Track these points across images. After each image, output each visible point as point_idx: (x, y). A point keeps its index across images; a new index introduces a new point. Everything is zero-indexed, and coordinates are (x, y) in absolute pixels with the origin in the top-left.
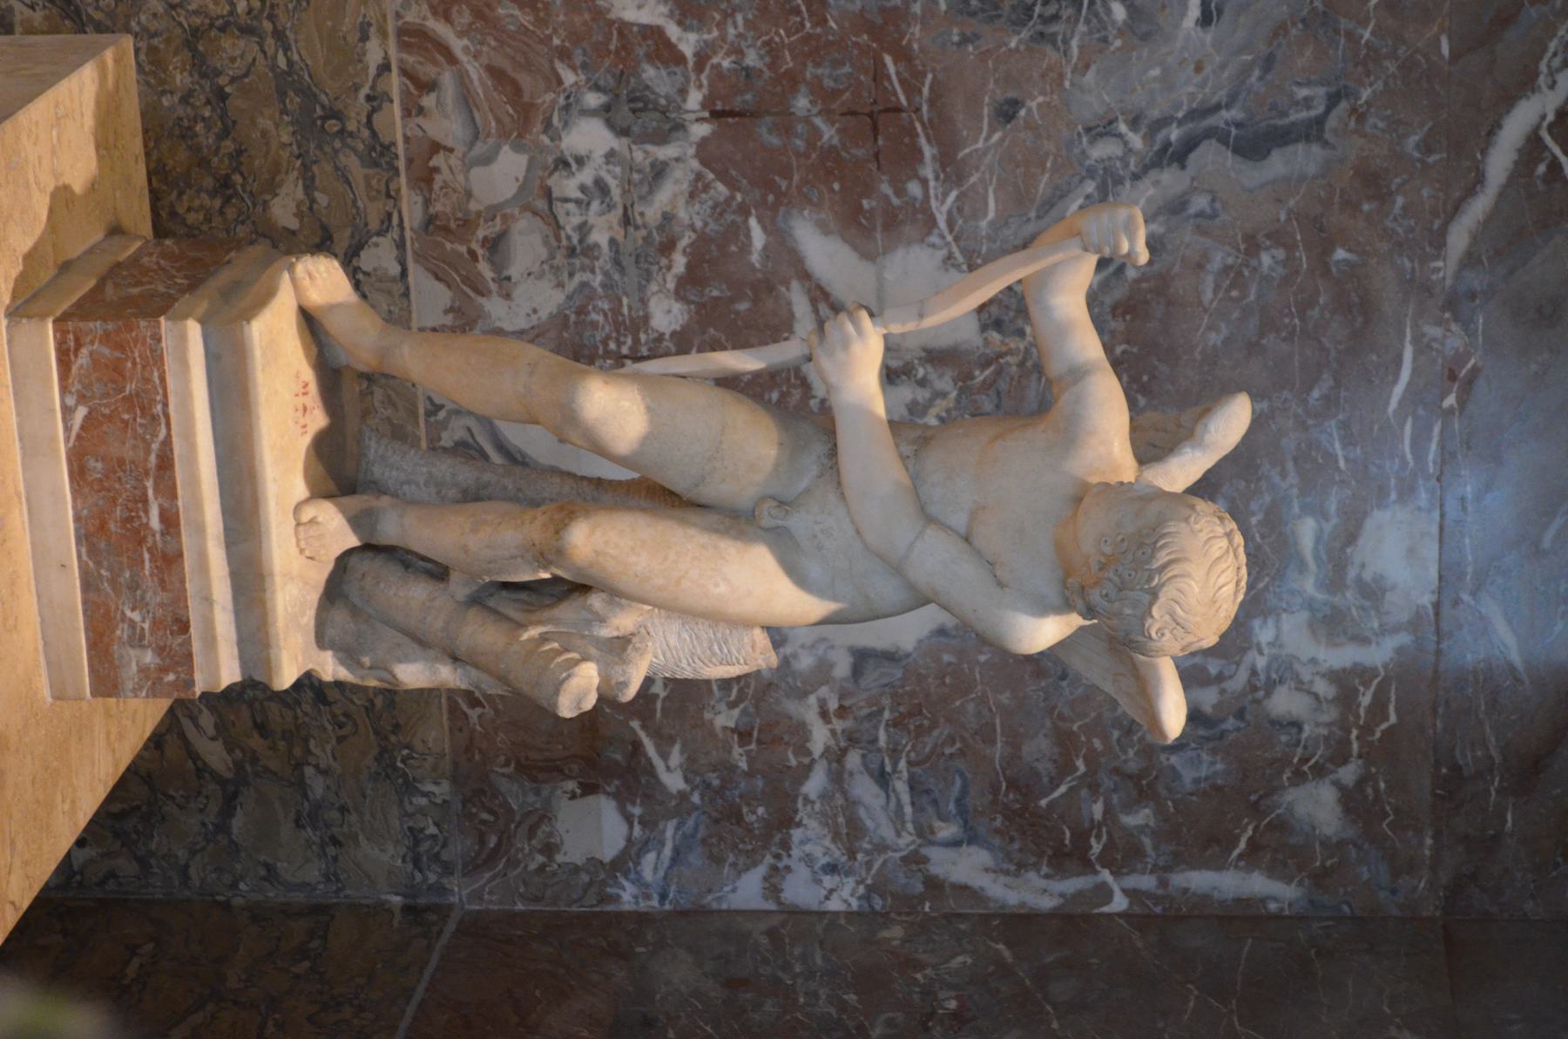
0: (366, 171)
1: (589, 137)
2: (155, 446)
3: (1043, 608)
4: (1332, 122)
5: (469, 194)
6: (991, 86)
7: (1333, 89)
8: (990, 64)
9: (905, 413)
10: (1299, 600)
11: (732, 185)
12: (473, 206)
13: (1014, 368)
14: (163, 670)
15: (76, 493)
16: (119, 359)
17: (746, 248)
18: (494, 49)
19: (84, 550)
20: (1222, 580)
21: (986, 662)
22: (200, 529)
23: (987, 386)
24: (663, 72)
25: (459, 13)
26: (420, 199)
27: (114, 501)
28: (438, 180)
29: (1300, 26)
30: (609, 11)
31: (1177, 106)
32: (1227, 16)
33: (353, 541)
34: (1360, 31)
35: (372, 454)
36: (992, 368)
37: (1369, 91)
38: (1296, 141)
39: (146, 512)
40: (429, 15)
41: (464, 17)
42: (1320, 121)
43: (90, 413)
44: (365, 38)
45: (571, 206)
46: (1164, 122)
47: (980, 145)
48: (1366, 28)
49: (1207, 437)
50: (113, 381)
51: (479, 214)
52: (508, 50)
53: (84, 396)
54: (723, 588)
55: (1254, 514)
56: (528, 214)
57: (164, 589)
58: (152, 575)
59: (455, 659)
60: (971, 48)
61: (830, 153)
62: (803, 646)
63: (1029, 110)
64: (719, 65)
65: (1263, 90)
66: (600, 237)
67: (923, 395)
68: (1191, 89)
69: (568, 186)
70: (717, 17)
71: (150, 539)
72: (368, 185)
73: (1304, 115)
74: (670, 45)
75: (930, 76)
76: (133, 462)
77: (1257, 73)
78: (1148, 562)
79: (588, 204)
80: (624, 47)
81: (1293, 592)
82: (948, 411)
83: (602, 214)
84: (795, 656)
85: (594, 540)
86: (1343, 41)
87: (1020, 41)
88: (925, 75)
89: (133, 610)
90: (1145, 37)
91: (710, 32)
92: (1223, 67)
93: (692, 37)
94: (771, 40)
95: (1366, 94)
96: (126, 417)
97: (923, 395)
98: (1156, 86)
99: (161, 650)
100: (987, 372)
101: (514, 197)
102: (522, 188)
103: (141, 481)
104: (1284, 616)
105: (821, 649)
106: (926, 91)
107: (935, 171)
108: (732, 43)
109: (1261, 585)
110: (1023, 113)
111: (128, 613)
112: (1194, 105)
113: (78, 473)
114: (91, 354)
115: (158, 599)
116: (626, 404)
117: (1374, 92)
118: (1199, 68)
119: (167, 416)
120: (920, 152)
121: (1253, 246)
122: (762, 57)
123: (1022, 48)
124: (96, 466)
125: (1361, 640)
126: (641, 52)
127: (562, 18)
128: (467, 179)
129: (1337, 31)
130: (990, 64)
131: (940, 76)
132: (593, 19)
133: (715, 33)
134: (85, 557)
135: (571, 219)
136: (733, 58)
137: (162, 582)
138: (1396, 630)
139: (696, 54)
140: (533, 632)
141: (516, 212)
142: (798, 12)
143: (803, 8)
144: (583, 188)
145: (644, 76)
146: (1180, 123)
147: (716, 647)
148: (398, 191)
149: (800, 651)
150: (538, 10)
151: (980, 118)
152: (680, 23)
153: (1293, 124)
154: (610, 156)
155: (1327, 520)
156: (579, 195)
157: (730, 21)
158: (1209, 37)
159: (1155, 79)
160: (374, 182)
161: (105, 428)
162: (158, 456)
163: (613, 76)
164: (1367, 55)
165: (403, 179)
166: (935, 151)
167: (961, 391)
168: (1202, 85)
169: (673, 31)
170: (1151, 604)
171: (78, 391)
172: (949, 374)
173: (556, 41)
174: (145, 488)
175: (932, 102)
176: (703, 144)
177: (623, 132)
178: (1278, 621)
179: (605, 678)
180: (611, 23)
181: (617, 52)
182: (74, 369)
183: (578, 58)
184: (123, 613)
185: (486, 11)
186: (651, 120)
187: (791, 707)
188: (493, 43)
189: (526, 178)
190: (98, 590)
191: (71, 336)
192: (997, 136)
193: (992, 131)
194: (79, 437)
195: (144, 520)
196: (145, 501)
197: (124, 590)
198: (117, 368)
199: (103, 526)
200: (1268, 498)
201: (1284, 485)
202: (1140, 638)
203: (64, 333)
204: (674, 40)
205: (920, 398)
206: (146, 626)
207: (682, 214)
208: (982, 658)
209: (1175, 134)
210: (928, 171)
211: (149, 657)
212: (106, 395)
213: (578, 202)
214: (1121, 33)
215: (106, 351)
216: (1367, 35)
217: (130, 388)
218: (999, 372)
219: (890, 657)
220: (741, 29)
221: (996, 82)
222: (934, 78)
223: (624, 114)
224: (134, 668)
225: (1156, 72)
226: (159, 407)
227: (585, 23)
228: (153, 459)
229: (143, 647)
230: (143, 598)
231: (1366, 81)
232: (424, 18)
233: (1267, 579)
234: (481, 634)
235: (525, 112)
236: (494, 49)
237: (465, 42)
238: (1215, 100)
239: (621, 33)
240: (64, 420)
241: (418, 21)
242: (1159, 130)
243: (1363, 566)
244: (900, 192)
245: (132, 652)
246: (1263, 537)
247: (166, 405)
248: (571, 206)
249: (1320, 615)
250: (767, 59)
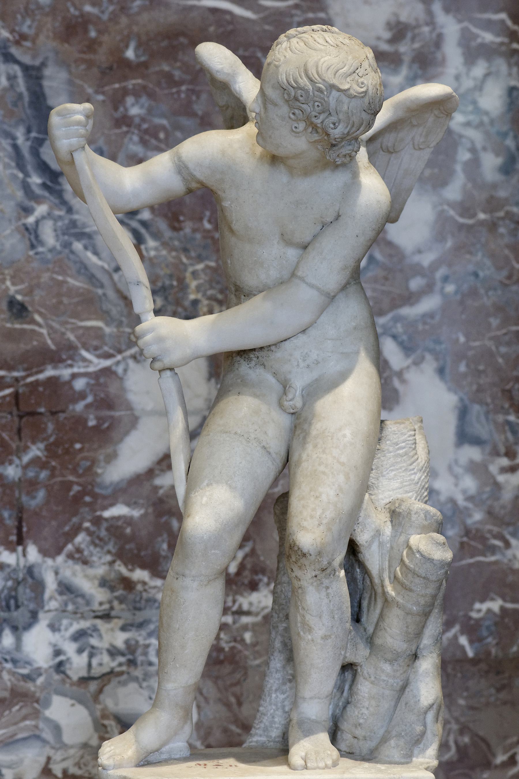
1: (38, 644)
3: (353, 185)
4: (27, 60)
11: (77, 530)
17: (128, 521)
20: (321, 41)
31: (15, 177)
33: (324, 737)
35: (263, 739)
38: (41, 86)
42: (26, 68)
45: (95, 662)
47: (44, 331)
49: (226, 71)
54: (347, 432)
56: (102, 697)
59: (415, 657)
61: (51, 450)
62: (456, 485)
66: (120, 639)
69: (78, 663)
78: (307, 91)
79: (93, 647)
83: (100, 636)
84: (464, 492)
85: (312, 526)
101: (87, 707)
102: (81, 702)
105: (459, 470)
110: (19, 297)
112: (13, 164)
116: (205, 499)
121: (125, 121)
125: (438, 42)
128: (72, 747)
135: (105, 662)
138: (430, 13)
140: (390, 590)
141: (99, 707)
144: (80, 651)
146: (27, 175)
147: (401, 452)
151: (24, 331)
153: (28, 89)
154: (53, 627)
156: (85, 655)
166: (49, 367)
170: (339, 90)
175: (10, 368)
176: (44, 552)
177: (34, 617)
179: (424, 530)
186: (25, 593)
187: (507, 496)
189: (72, 698)
192: (37, 318)
193: (33, 322)
202: (366, 100)
207: (101, 571)
208: (462, 339)
209: (36, 180)
210: (65, 373)
213: (91, 656)
219: (463, 413)
223: (20, 615)
234: (393, 633)
235: (18, 695)
238: (9, 149)
242: (32, 192)
243: (379, 38)
244: (82, 395)
248: (95, 662)
249: (420, 72)
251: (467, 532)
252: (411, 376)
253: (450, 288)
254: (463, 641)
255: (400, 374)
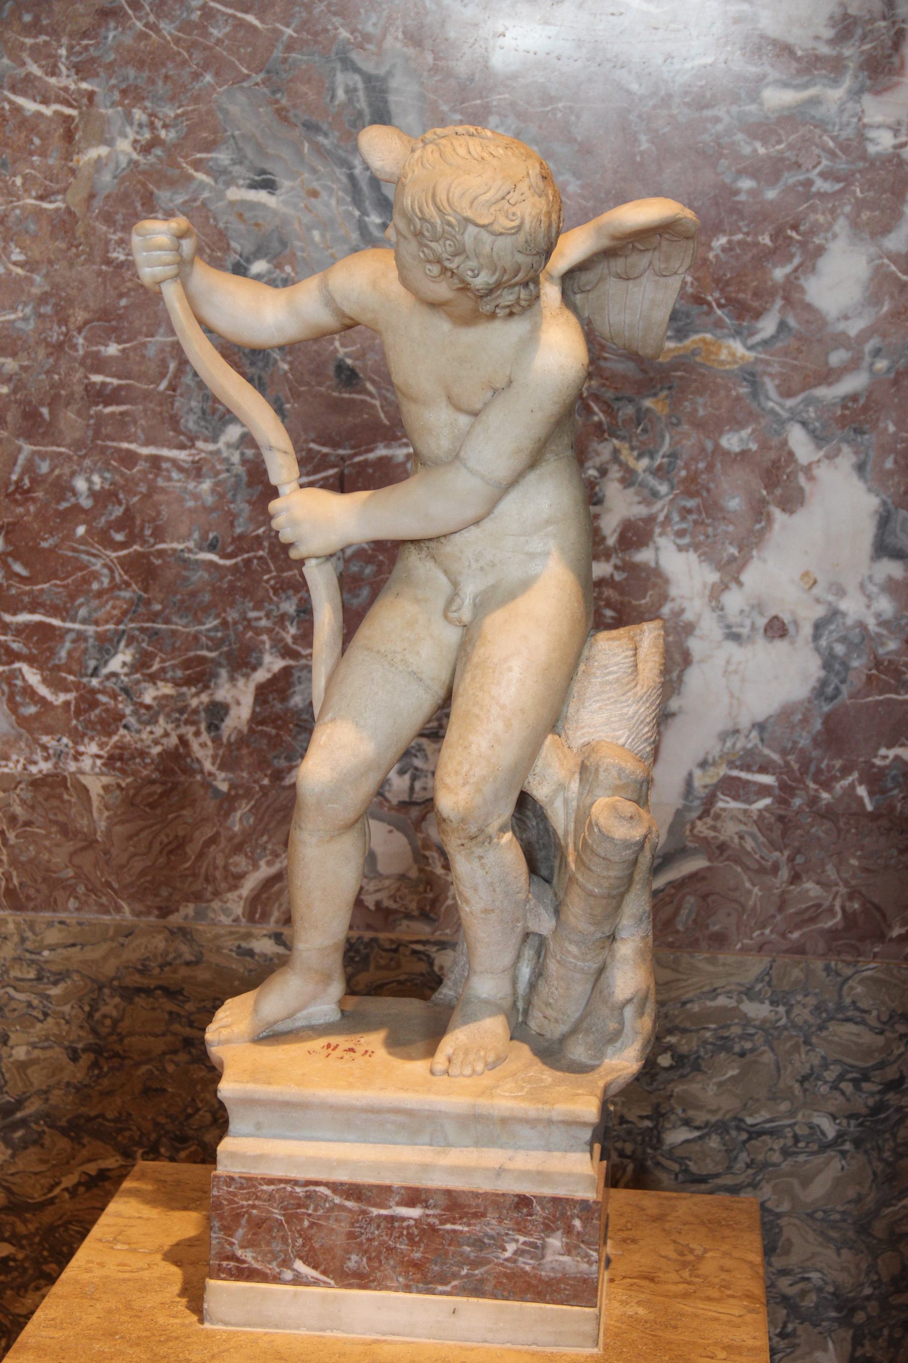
0: (372, 967)
2: (337, 1200)
3: (531, 340)
5: (402, 877)
6: (323, 389)
7: (339, 66)
8: (302, 389)
9: (631, 490)
10: (850, 105)
12: (414, 874)
13: (593, 383)
14: (569, 1230)
15: (381, 1287)
16: (248, 1221)
18: (270, 838)
19: (440, 1288)
20: (462, 151)
21: (895, 424)
22: (425, 1168)
23: (609, 410)
24: (298, 688)
25: (236, 865)
26: (405, 923)
27: (390, 1249)
28: (387, 903)
29: (278, 96)
30: (240, 732)
31: (350, 215)
32: (268, 166)
34: (285, 38)
35: (452, 993)
36: (592, 404)
37: (341, 30)
38: (386, 102)
39: (403, 1219)
40: (237, 893)
41: (240, 862)
43: (301, 1258)
44: (250, 953)
45: (418, 785)
46: (362, 227)
47: (377, 403)
48: (282, 33)
49: (388, 169)
50: (270, 1230)
51: (421, 870)
52: (272, 826)
53: (284, 1261)
55: (755, 151)
56: (423, 825)
57: (483, 1215)
58: (469, 1225)
59: (612, 938)
60: (288, 406)
62: (868, 607)
63: (347, 355)
64: (294, 637)
65: (337, 134)
67: (615, 472)
68: (333, 202)
70: (250, 634)
71: (431, 1220)
72: (386, 967)
73: (361, 94)
74: (274, 679)
75: (312, 445)
76: (352, 1225)
77: (321, 139)
78: (433, 226)
79: (416, 769)
80: (274, 721)
81: (842, 111)
82: (632, 448)
83: (426, 757)
84: (878, 615)
86: (293, 55)
87: (283, 360)
88: (310, 450)
89: (504, 1250)
90: (284, 243)
91: (263, 643)
92: (314, 171)
93: (267, 659)
94: (273, 588)
95: (344, 34)
96: (306, 1223)
97: (615, 472)
98: (328, 236)
99: (548, 1228)
100: (596, 409)
101: (407, 835)
102: (399, 828)
103: (371, 1219)
104: (866, 120)
105: (873, 589)
106: (325, 450)
107: (400, 446)
108: (275, 623)
109: (831, 144)
110: (349, 361)
111: (507, 1254)
112: (349, 199)
113: (362, 1280)
114: (242, 1247)
115: (494, 1222)
116: (324, 738)
117: (342, 25)
118: (314, 194)
119: (308, 1183)
120: (381, 459)
122: (288, 598)
123: (289, 358)
124: (354, 1261)
126: (279, 706)
127: (245, 774)
128: (387, 877)
129: (285, 61)
130: (302, 389)
131: (313, 435)
132: (248, 746)
133: (265, 637)
134: (448, 1288)
136: (288, 623)
137: (475, 1215)
139: (283, 656)
141: (420, 835)
142: (248, 562)
143: (246, 556)
144: (401, 772)
145: (301, 705)
146: (364, 213)
147: (611, 677)
148: (392, 941)
149: (873, 610)
150: (237, 795)
151: (353, 401)
152: (254, 669)
153: (370, 105)
155: (765, 76)
156: (407, 777)
157: (254, 624)
158: (286, 183)
159: (323, 236)
160: (382, 962)
161: (317, 1246)
162: (347, 1199)
163: (299, 733)
164: (308, 32)
165: (382, 936)
166: (381, 445)
167: (613, 435)
168: (330, 191)
169: (261, 676)
170: (476, 225)
171: (279, 1266)
172: (595, 445)
173: (266, 782)
174: (379, 1216)
175: (336, 445)
178: (871, 126)
180: (252, 731)
181: (278, 728)
182: (256, 1265)
183: (282, 763)
184: (506, 1260)
185: (236, 841)
188: (265, 838)
189: (389, 824)
190: (482, 1281)
191: (225, 1263)
192: (370, 386)
193: (365, 391)
194: (324, 1273)
195: (412, 1222)
196: (392, 1219)
197: (482, 1254)
198: (257, 1225)
199: (416, 1265)
200: (740, 137)
201: (726, 119)
202: (521, 237)
203: (220, 1269)
204: (269, 676)
205: (619, 475)
206: (522, 1239)
208: (892, 428)
211: (556, 1242)
212: (284, 1239)
213: (414, 778)
214: (279, 266)
215: (240, 1232)
216: (289, 31)
217: (277, 1214)
218: (597, 398)
219: (884, 521)
220: (261, 614)
221: (320, 384)
222: (314, 441)
224: (566, 1258)
225: (316, 235)
226: (298, 1189)
227: (251, 754)
228: (349, 1204)
229: (544, 1247)
230: (491, 1237)
231: (332, 33)
232: (240, 897)
233: (825, 138)
236: (270, 838)
237: (262, 863)
238: (344, 179)
239: (262, 723)
240: (308, 1284)
241: (242, 903)
242: (370, 234)
243: (817, 38)
245: (549, 1258)
246: (779, 142)
247: (296, 1183)
248: (418, 785)
249: (868, 83)
250: (291, 592)
251: (878, 663)
252: (823, 472)
253: (882, 364)
254: (862, 791)
255: (808, 470)
